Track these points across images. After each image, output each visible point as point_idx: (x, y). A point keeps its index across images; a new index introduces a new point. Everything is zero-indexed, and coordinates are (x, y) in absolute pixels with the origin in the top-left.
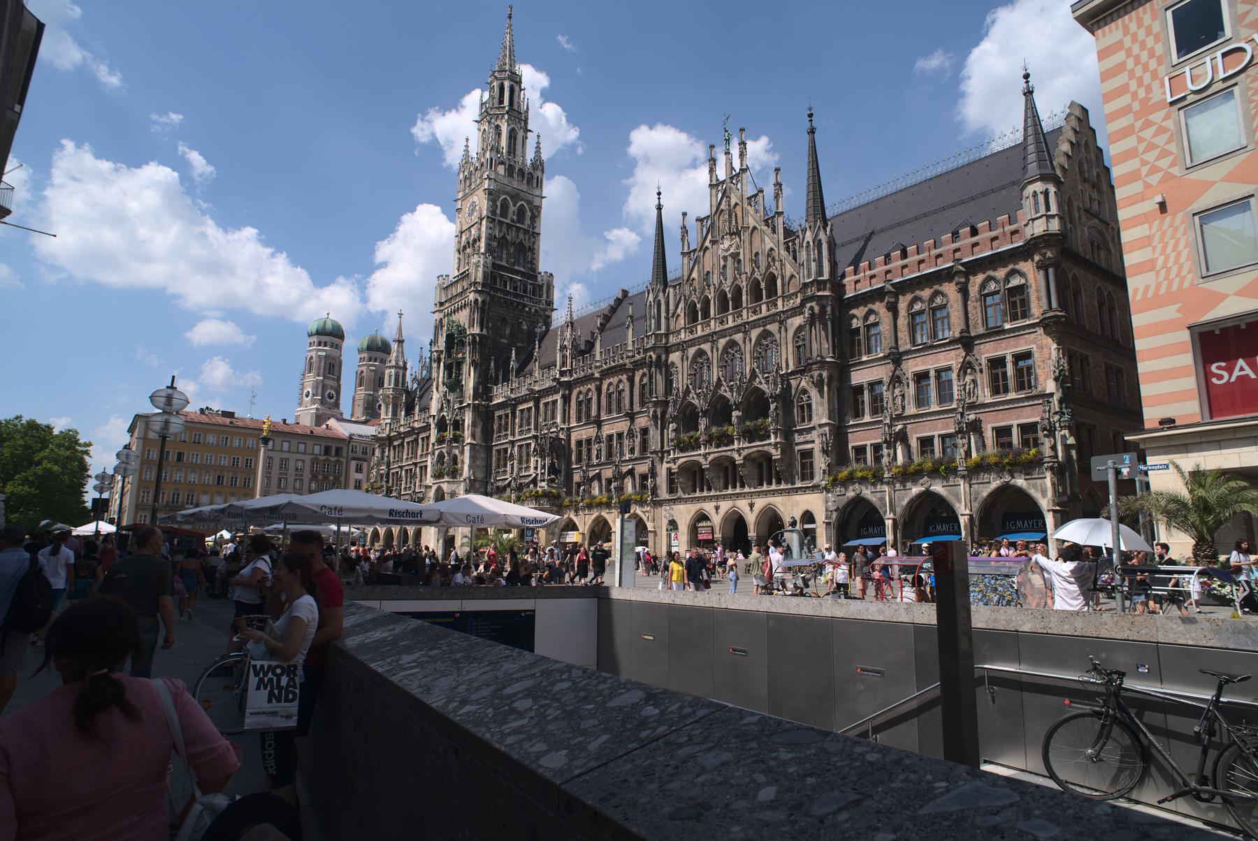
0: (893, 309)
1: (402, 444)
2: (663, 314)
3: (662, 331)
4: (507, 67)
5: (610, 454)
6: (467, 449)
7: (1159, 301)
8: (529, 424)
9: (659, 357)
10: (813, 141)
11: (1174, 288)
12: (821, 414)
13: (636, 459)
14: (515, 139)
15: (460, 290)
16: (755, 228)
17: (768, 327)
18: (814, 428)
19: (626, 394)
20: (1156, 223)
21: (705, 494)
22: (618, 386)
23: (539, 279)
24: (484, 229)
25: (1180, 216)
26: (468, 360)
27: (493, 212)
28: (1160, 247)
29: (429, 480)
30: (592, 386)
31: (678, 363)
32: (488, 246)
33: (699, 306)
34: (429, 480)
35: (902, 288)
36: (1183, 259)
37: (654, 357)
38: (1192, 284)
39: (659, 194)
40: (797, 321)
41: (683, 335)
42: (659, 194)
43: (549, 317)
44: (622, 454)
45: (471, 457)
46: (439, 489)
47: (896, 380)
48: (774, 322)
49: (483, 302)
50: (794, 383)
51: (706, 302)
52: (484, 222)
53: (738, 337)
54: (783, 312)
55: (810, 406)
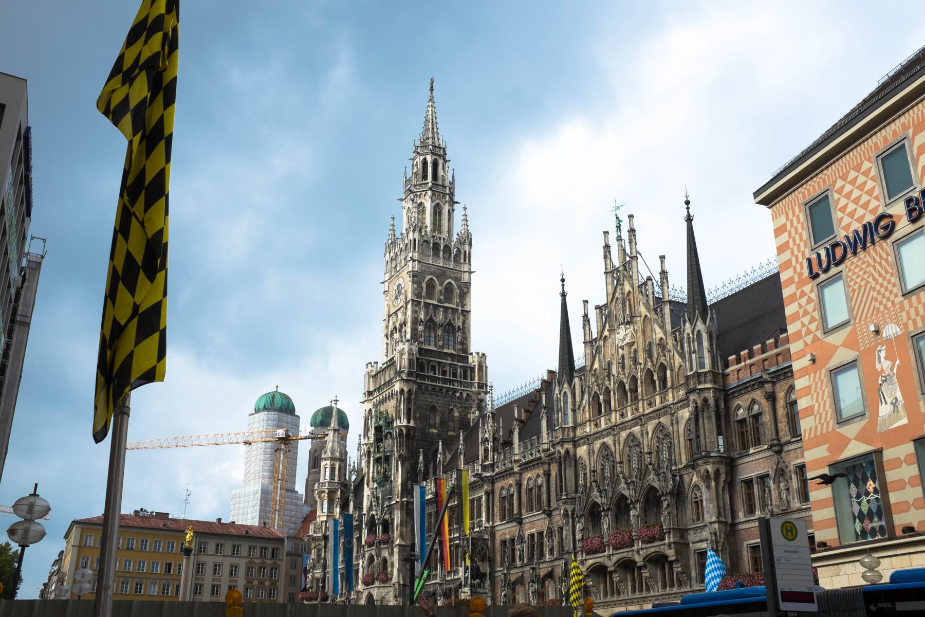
0: (772, 398)
3: (570, 425)
4: (430, 141)
5: (531, 558)
6: (396, 550)
7: (817, 442)
9: (567, 452)
11: (824, 432)
12: (710, 516)
13: (555, 560)
14: (440, 214)
15: (387, 379)
17: (662, 420)
18: (706, 526)
19: (544, 489)
20: (812, 375)
21: (615, 599)
22: (536, 481)
23: (470, 360)
24: (409, 313)
25: (823, 371)
26: (396, 454)
27: (419, 295)
29: (360, 587)
30: (511, 481)
32: (414, 330)
33: (601, 397)
34: (360, 587)
36: (827, 408)
37: (562, 451)
38: (833, 429)
39: (563, 280)
40: (685, 414)
41: (588, 429)
42: (563, 280)
43: (481, 401)
44: (542, 555)
45: (399, 559)
47: (781, 473)
48: (665, 413)
49: (409, 391)
50: (686, 479)
51: (608, 391)
52: (409, 306)
53: (637, 429)
54: (673, 404)
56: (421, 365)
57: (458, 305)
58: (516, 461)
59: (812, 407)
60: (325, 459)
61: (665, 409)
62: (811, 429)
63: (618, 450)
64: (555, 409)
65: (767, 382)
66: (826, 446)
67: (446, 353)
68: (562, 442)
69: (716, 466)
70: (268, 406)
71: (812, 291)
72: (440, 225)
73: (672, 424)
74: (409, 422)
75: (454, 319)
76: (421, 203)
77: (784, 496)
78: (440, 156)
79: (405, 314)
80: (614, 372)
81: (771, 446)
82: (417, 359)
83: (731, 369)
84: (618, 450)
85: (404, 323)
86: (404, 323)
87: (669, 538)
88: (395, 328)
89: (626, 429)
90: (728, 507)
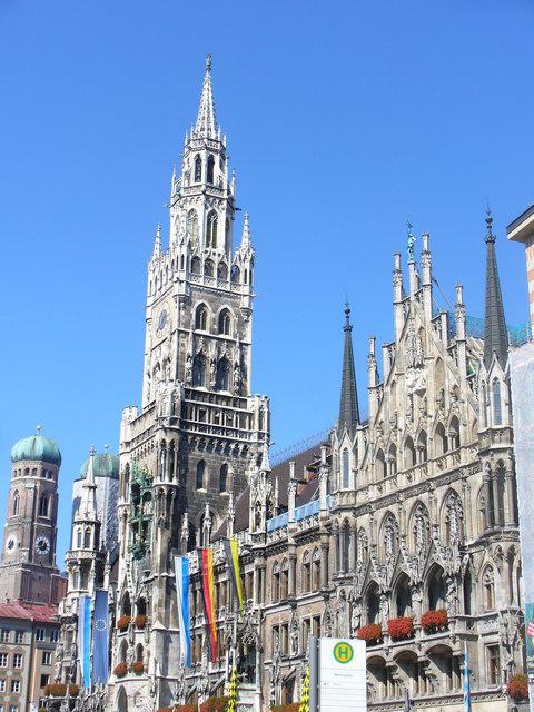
2: (351, 466)
3: (351, 488)
6: (153, 635)
9: (346, 520)
10: (492, 254)
14: (215, 223)
17: (453, 485)
24: (174, 346)
26: (156, 520)
27: (187, 325)
31: (367, 527)
33: (386, 456)
37: (341, 521)
39: (348, 312)
40: (478, 479)
45: (157, 647)
46: (122, 692)
49: (172, 441)
50: (476, 556)
51: (393, 449)
52: (175, 337)
53: (424, 497)
58: (291, 531)
60: (79, 523)
61: (455, 474)
67: (219, 396)
70: (27, 454)
72: (215, 238)
76: (192, 210)
78: (216, 151)
79: (170, 347)
80: (401, 425)
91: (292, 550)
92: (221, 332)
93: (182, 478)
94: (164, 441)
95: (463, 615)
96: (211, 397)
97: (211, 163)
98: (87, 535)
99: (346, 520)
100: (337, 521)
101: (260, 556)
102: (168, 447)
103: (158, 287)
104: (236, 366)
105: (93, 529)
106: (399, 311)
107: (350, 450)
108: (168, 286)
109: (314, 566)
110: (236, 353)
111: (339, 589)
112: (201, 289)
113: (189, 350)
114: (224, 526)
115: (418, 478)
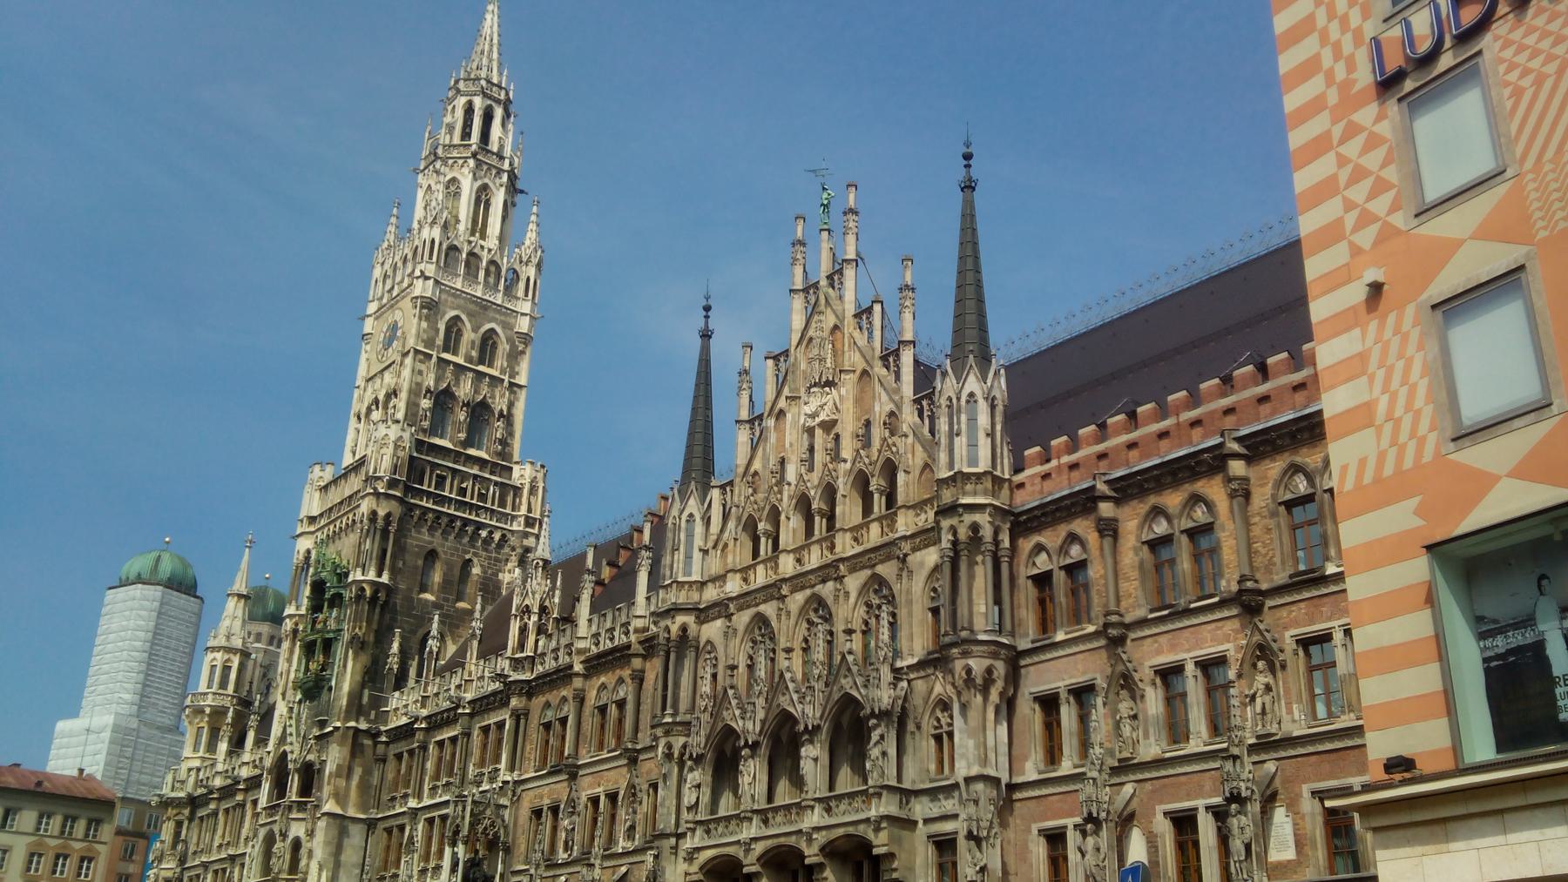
0: (1109, 530)
1: (215, 814)
2: (698, 541)
3: (695, 577)
6: (322, 824)
7: (1382, 493)
8: (451, 774)
9: (684, 628)
14: (488, 204)
15: (347, 493)
16: (865, 373)
17: (880, 569)
24: (406, 373)
25: (1410, 310)
26: (346, 636)
27: (430, 343)
28: (1380, 374)
32: (412, 406)
33: (761, 526)
35: (1128, 489)
36: (1419, 402)
37: (674, 629)
38: (1438, 455)
40: (931, 557)
44: (611, 839)
45: (327, 843)
48: (889, 558)
49: (388, 515)
51: (775, 515)
52: (408, 361)
54: (904, 538)
55: (951, 735)
56: (416, 468)
57: (503, 371)
58: (579, 652)
59: (1368, 408)
60: (213, 649)
61: (886, 550)
62: (1363, 462)
63: (784, 628)
64: (669, 545)
65: (1105, 498)
66: (1414, 502)
67: (469, 457)
68: (674, 610)
69: (987, 662)
71: (1380, 118)
73: (899, 576)
74: (379, 575)
75: (493, 397)
76: (454, 180)
77: (1126, 730)
78: (498, 101)
81: (1106, 626)
82: (411, 457)
83: (1028, 472)
84: (784, 628)
85: (393, 393)
86: (393, 393)
87: (878, 807)
88: (376, 401)
89: (803, 588)
90: (1004, 749)
91: (578, 683)
92: (481, 362)
93: (394, 572)
94: (374, 513)
95: (894, 783)
96: (457, 456)
97: (488, 117)
98: (226, 669)
99: (684, 628)
100: (667, 629)
101: (520, 695)
102: (380, 522)
103: (388, 287)
104: (501, 415)
105: (236, 661)
106: (798, 303)
107: (698, 517)
108: (405, 285)
109: (613, 711)
110: (502, 396)
111: (662, 742)
112: (456, 294)
113: (430, 381)
114: (462, 652)
115: (814, 559)
